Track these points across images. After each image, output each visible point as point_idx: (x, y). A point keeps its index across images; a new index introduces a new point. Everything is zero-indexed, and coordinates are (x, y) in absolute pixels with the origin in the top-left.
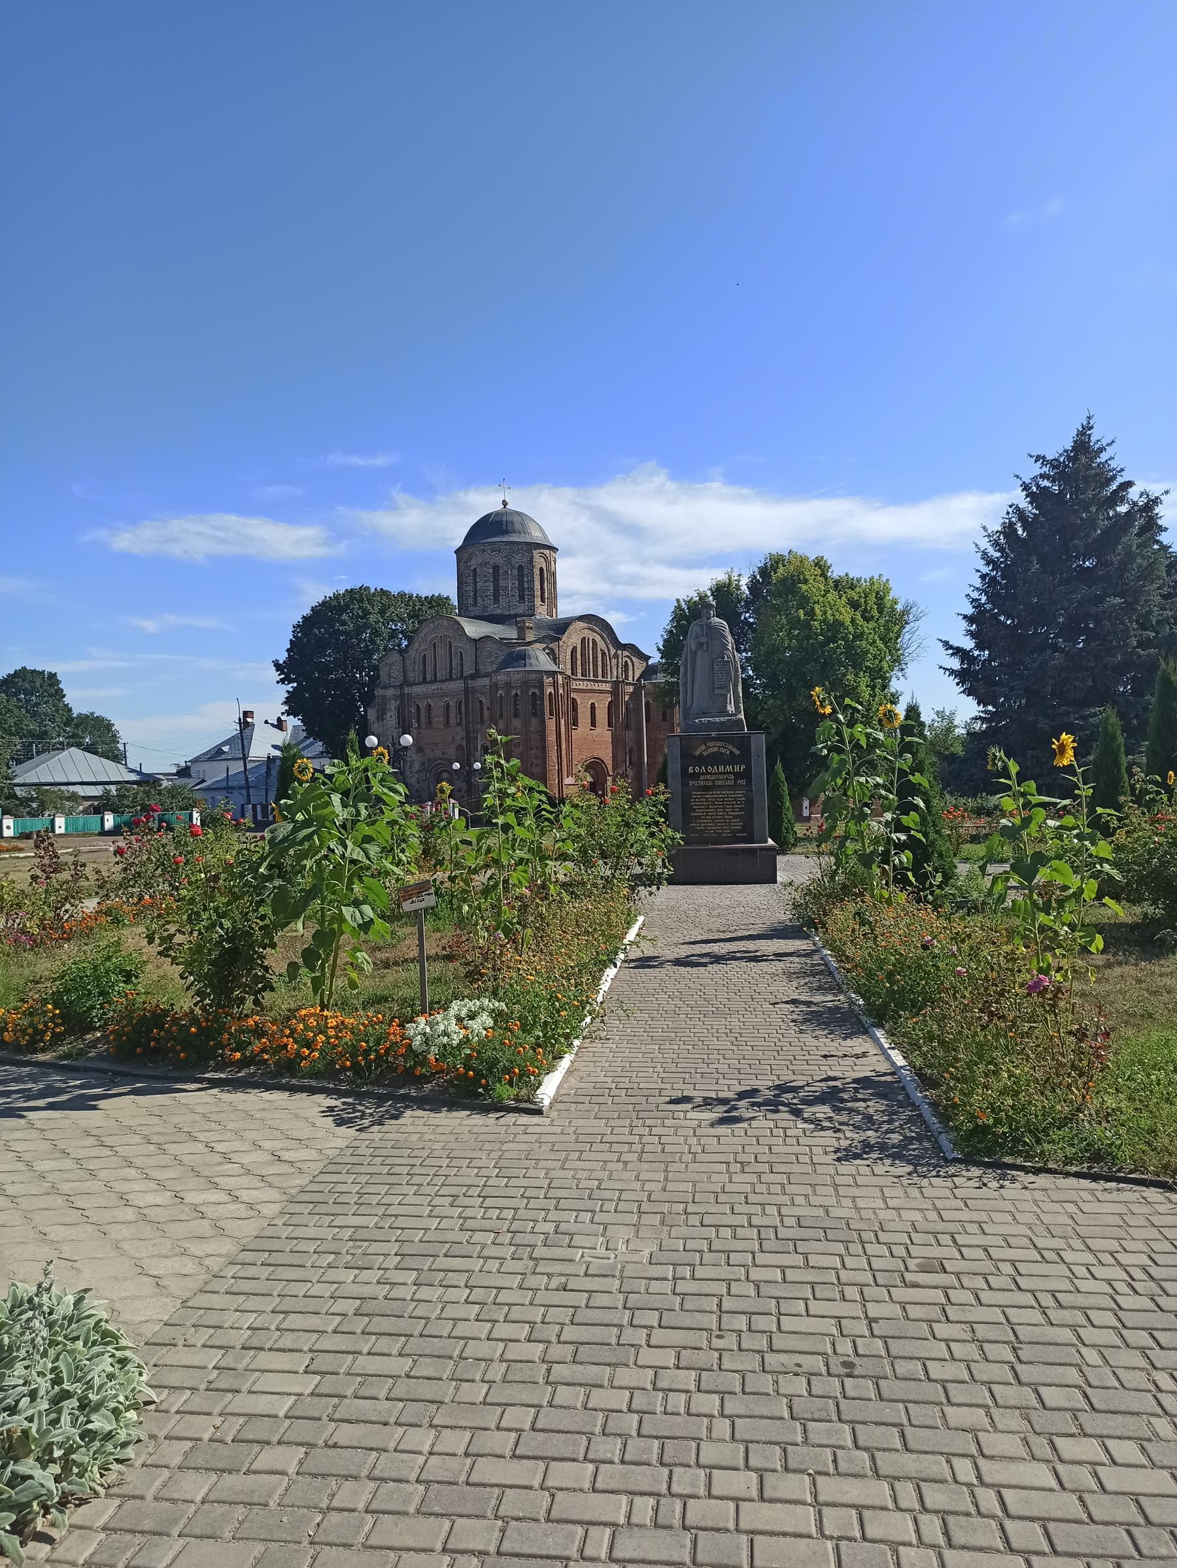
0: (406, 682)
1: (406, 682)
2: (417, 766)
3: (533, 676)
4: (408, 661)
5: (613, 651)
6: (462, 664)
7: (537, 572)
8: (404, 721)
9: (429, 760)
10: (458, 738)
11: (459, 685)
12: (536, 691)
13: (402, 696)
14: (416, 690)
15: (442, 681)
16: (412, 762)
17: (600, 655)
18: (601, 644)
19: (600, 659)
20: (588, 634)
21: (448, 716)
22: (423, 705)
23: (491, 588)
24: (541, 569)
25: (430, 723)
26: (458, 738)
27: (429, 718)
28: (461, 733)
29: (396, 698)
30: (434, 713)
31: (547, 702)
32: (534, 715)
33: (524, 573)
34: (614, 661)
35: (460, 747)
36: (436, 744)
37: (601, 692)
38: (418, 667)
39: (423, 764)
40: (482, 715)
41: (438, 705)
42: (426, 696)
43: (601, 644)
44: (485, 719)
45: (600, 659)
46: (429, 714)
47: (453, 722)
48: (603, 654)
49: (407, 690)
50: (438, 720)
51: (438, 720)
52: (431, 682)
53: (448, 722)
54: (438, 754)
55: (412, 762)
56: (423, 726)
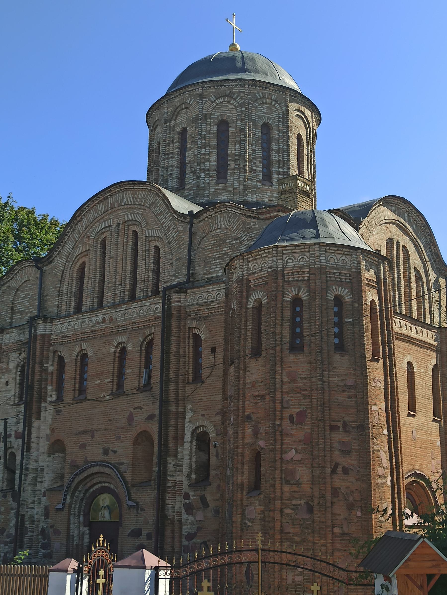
0: (43, 315)
1: (43, 315)
2: (47, 480)
3: (338, 259)
4: (49, 280)
5: (433, 277)
6: (157, 273)
7: (293, 140)
8: (30, 388)
9: (74, 466)
10: (140, 417)
11: (155, 306)
12: (344, 292)
13: (32, 339)
14: (60, 328)
15: (114, 306)
16: (39, 471)
17: (413, 279)
18: (415, 260)
19: (414, 285)
20: (395, 233)
21: (121, 374)
22: (70, 355)
23: (213, 158)
24: (299, 137)
25: (82, 391)
26: (140, 417)
27: (82, 380)
28: (149, 405)
29: (20, 346)
30: (92, 369)
31: (367, 321)
32: (340, 348)
33: (272, 136)
34: (435, 295)
35: (143, 437)
36: (92, 433)
37: (423, 344)
38: (69, 287)
39: (60, 477)
40: (197, 366)
41: (101, 355)
42: (83, 337)
43: (415, 260)
44: (205, 373)
45: (414, 285)
46: (83, 372)
47: (131, 382)
48: (419, 278)
49: (42, 328)
50: (100, 382)
51: (100, 382)
52: (92, 310)
53: (120, 385)
54: (95, 453)
55: (39, 471)
56: (68, 397)
